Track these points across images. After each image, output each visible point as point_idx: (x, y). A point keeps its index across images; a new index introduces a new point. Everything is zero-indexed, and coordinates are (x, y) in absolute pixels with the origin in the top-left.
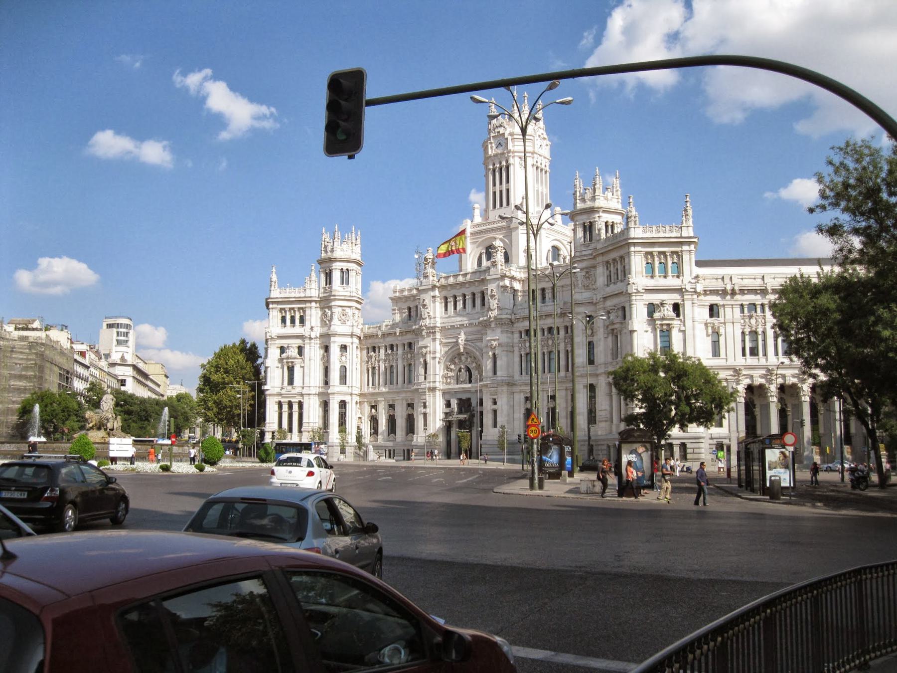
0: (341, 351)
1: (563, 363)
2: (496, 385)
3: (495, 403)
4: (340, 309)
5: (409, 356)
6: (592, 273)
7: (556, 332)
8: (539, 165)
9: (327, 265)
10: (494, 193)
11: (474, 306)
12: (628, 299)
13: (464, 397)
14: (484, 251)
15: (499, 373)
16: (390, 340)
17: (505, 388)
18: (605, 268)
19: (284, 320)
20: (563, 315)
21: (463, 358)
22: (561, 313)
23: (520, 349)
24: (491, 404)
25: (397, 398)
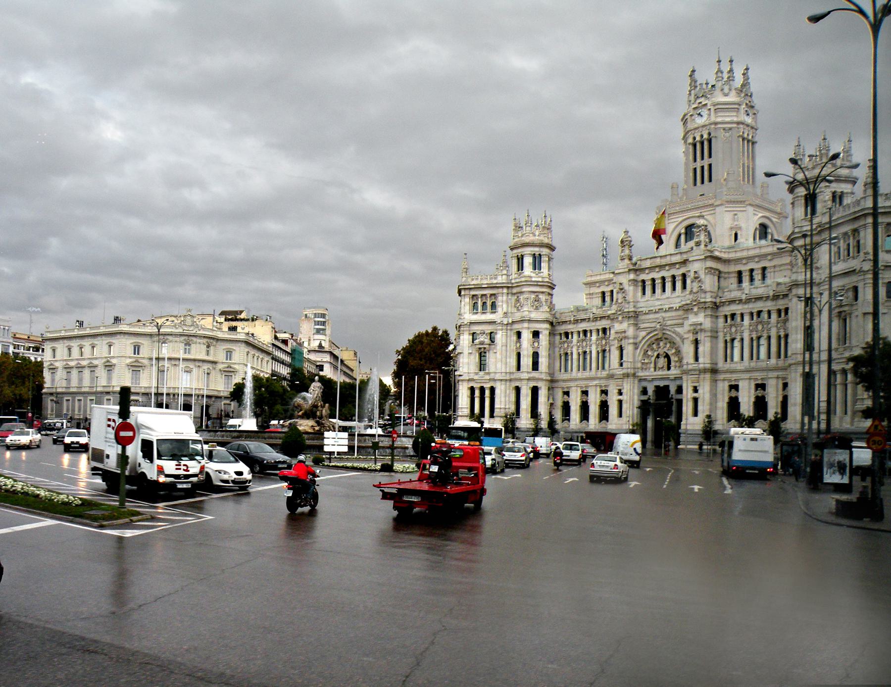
0: (533, 337)
1: (774, 349)
2: (698, 373)
3: (696, 390)
4: (533, 296)
7: (766, 316)
8: (746, 136)
9: (520, 250)
10: (695, 169)
11: (674, 289)
13: (662, 384)
14: (683, 231)
15: (701, 360)
16: (583, 326)
19: (475, 306)
20: (776, 297)
21: (662, 344)
22: (774, 296)
24: (692, 392)
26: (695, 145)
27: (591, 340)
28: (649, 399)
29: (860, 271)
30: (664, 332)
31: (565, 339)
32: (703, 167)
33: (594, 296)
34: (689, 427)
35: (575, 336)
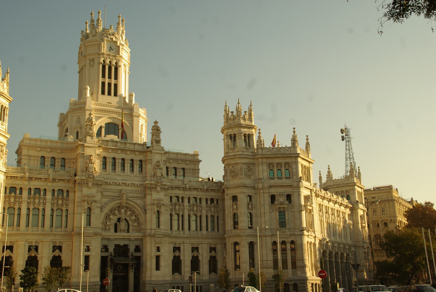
1: (204, 224)
2: (162, 237)
3: (158, 249)
5: (60, 202)
6: (251, 167)
10: (103, 84)
12: (297, 190)
13: (122, 243)
14: (104, 126)
15: (162, 227)
16: (35, 184)
17: (167, 239)
18: (268, 167)
21: (123, 211)
23: (171, 210)
25: (43, 240)
26: (104, 67)
27: (45, 199)
28: (111, 255)
29: (296, 187)
30: (127, 201)
31: (13, 194)
32: (110, 84)
33: (31, 158)
34: (153, 279)
35: (25, 194)
